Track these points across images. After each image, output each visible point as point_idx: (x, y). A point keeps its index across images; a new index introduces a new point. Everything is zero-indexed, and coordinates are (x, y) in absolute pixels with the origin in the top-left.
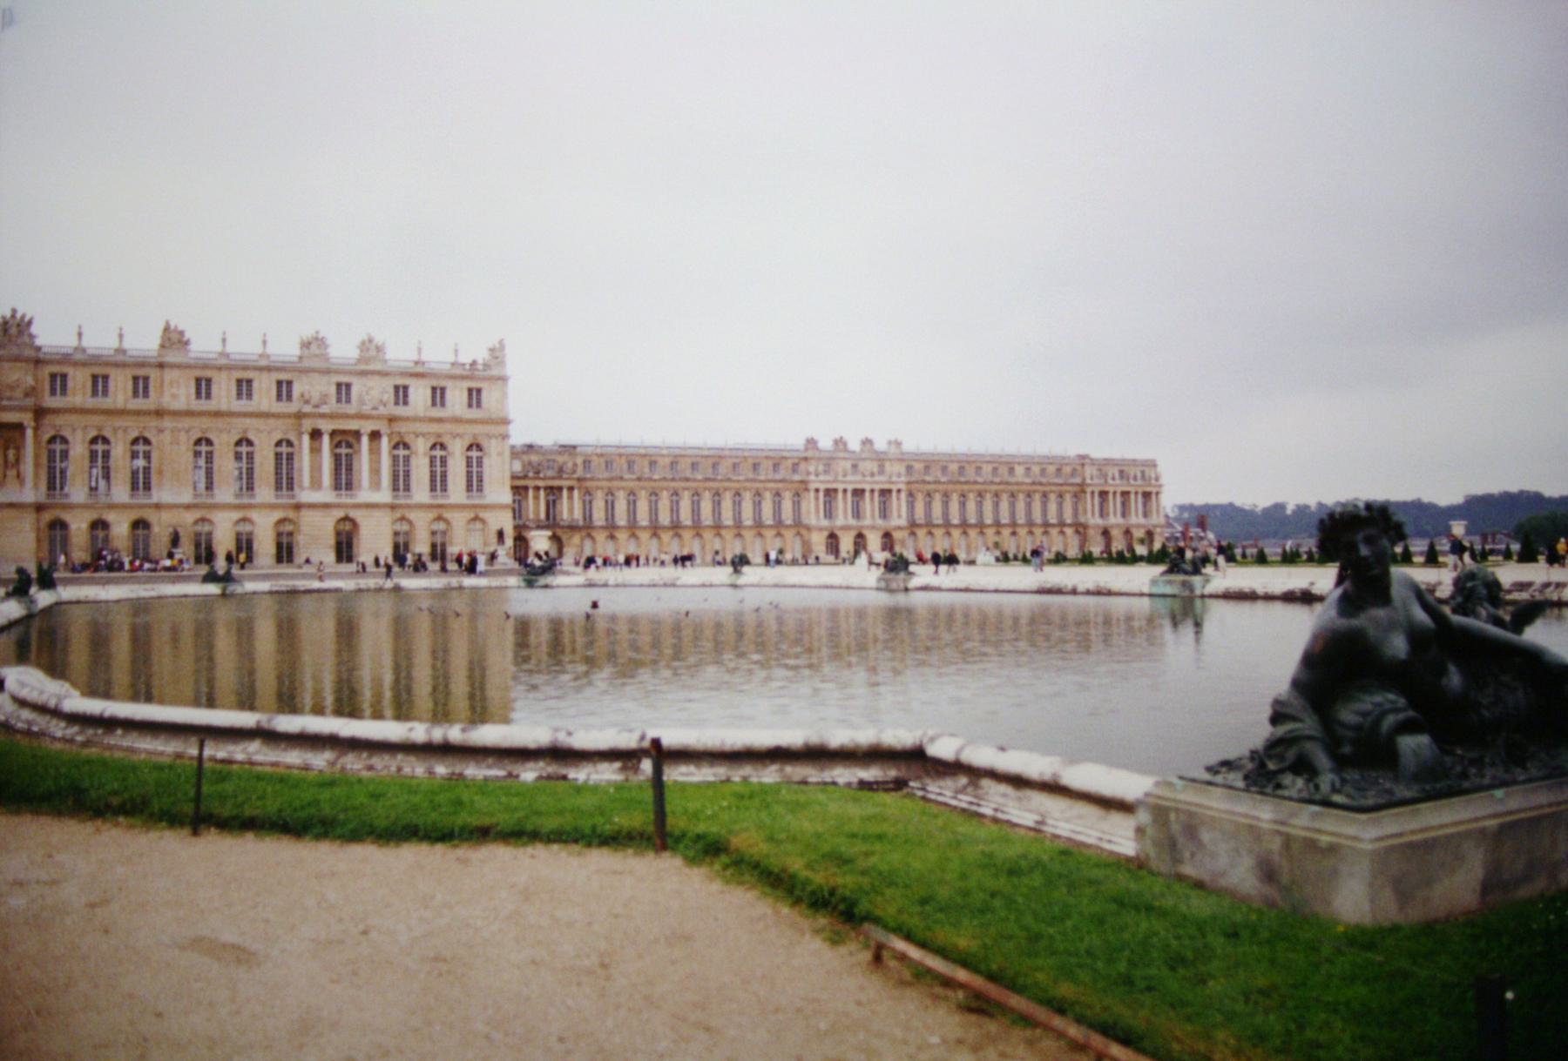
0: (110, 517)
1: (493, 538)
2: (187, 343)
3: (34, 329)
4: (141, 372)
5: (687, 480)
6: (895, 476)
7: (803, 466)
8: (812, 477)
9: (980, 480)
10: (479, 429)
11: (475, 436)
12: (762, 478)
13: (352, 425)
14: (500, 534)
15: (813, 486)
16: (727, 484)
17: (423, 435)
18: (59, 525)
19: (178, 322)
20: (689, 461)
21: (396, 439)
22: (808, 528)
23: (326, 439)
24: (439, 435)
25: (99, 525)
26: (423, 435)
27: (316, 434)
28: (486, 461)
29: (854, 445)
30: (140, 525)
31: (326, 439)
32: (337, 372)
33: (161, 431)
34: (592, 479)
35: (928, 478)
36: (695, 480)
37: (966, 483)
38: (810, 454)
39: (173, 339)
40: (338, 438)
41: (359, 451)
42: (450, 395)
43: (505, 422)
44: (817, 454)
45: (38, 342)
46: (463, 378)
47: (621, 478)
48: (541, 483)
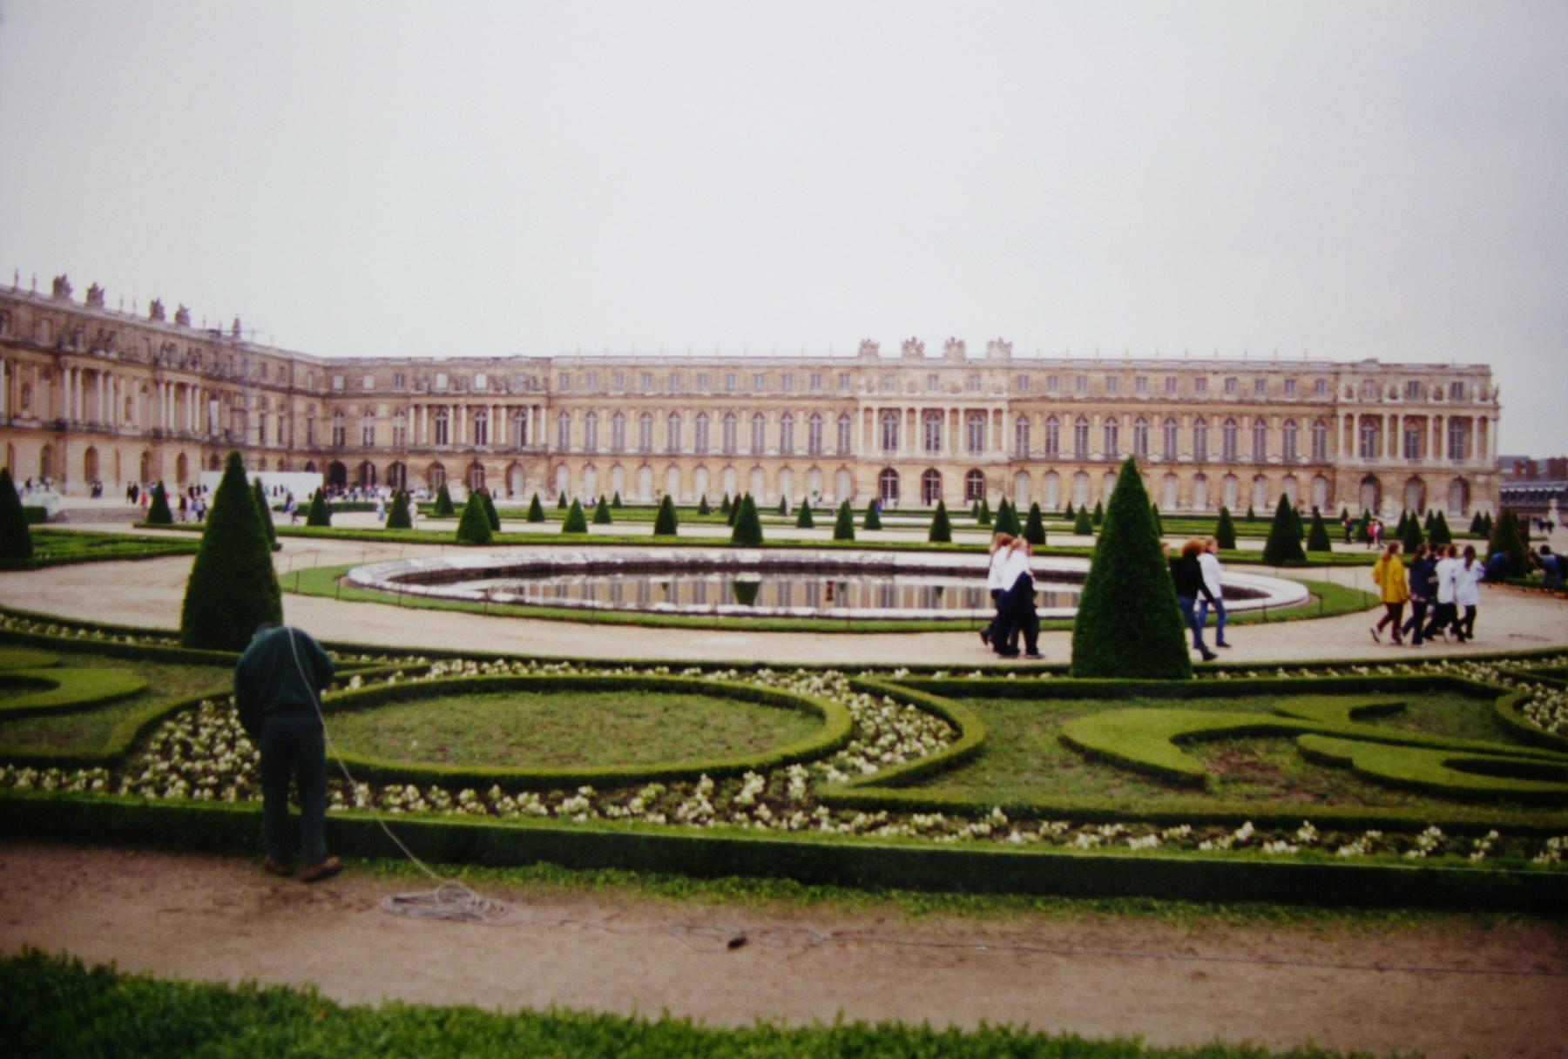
5: (689, 396)
6: (995, 391)
7: (854, 377)
8: (863, 393)
9: (1143, 396)
12: (795, 394)
15: (863, 404)
16: (743, 402)
20: (694, 372)
22: (854, 459)
29: (934, 349)
34: (567, 397)
35: (1053, 394)
36: (700, 397)
37: (1120, 400)
38: (864, 362)
44: (874, 362)
47: (605, 395)
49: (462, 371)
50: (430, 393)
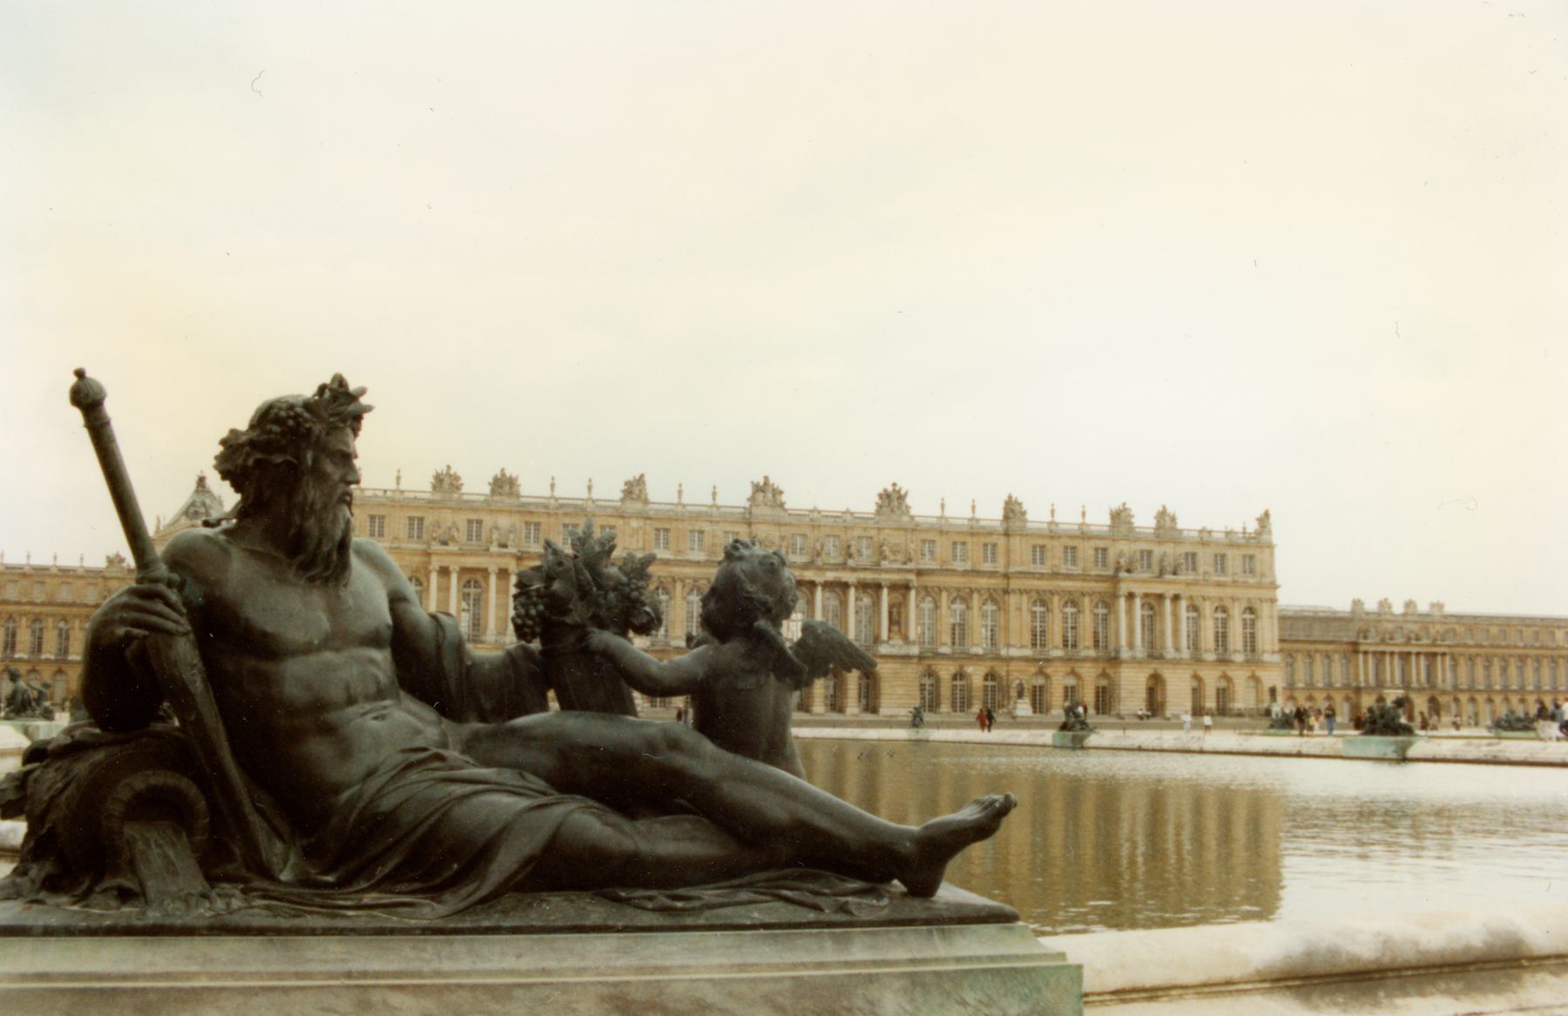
0: (970, 670)
1: (1267, 697)
2: (1024, 513)
3: (908, 501)
4: (989, 540)
10: (1252, 593)
13: (1157, 588)
14: (1273, 691)
18: (930, 673)
19: (1019, 495)
24: (1221, 599)
25: (959, 675)
28: (1259, 624)
30: (991, 676)
32: (1032, 535)
33: (1006, 592)
37: (1508, 647)
39: (1012, 510)
41: (1162, 615)
42: (1229, 563)
43: (1274, 586)
45: (913, 512)
46: (1239, 546)
48: (1396, 649)
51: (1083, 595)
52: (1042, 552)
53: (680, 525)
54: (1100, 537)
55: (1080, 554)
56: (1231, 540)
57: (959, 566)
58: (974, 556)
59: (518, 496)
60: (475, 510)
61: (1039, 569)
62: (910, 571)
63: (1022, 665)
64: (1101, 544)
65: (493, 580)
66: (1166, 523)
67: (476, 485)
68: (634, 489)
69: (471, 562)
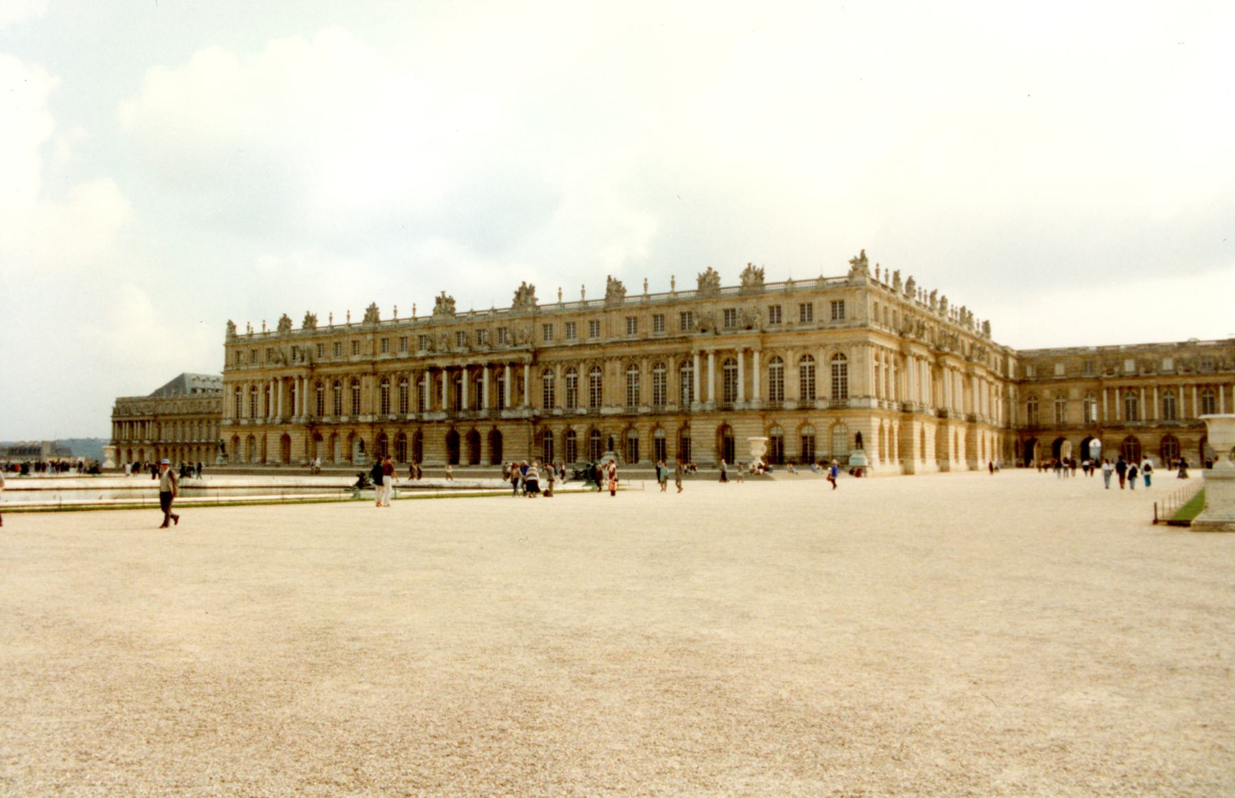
0: (575, 428)
2: (624, 291)
3: (536, 295)
11: (837, 345)
17: (792, 348)
21: (769, 355)
23: (711, 358)
24: (805, 347)
26: (792, 348)
27: (703, 355)
30: (594, 432)
31: (711, 358)
39: (615, 288)
40: (724, 357)
45: (538, 303)
46: (825, 293)
49: (1149, 356)
50: (1121, 377)
51: (668, 357)
52: (635, 322)
53: (393, 335)
54: (685, 302)
55: (667, 320)
56: (822, 286)
57: (570, 342)
58: (583, 332)
59: (314, 328)
60: (295, 340)
61: (632, 337)
62: (521, 351)
63: (614, 420)
64: (685, 309)
65: (297, 383)
66: (753, 280)
67: (297, 325)
68: (372, 312)
69: (287, 373)
